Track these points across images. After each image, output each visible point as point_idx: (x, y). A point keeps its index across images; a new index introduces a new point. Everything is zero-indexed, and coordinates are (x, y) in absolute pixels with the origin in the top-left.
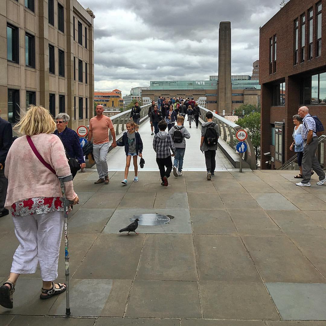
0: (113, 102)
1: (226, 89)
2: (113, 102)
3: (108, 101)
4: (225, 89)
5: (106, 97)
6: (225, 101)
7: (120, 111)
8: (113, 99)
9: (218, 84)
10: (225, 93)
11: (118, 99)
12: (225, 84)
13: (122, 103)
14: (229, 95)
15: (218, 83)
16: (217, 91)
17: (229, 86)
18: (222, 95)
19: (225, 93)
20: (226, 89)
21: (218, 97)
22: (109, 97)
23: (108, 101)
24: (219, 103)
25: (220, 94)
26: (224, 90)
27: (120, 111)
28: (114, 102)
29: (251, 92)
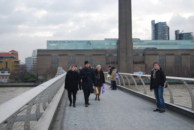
0: (7, 63)
1: (127, 49)
2: (7, 63)
4: (126, 48)
7: (10, 74)
8: (6, 60)
10: (127, 54)
11: (13, 60)
13: (18, 64)
15: (119, 43)
16: (118, 51)
19: (127, 54)
20: (128, 48)
21: (118, 57)
24: (120, 64)
27: (10, 74)
28: (8, 63)
29: (152, 52)
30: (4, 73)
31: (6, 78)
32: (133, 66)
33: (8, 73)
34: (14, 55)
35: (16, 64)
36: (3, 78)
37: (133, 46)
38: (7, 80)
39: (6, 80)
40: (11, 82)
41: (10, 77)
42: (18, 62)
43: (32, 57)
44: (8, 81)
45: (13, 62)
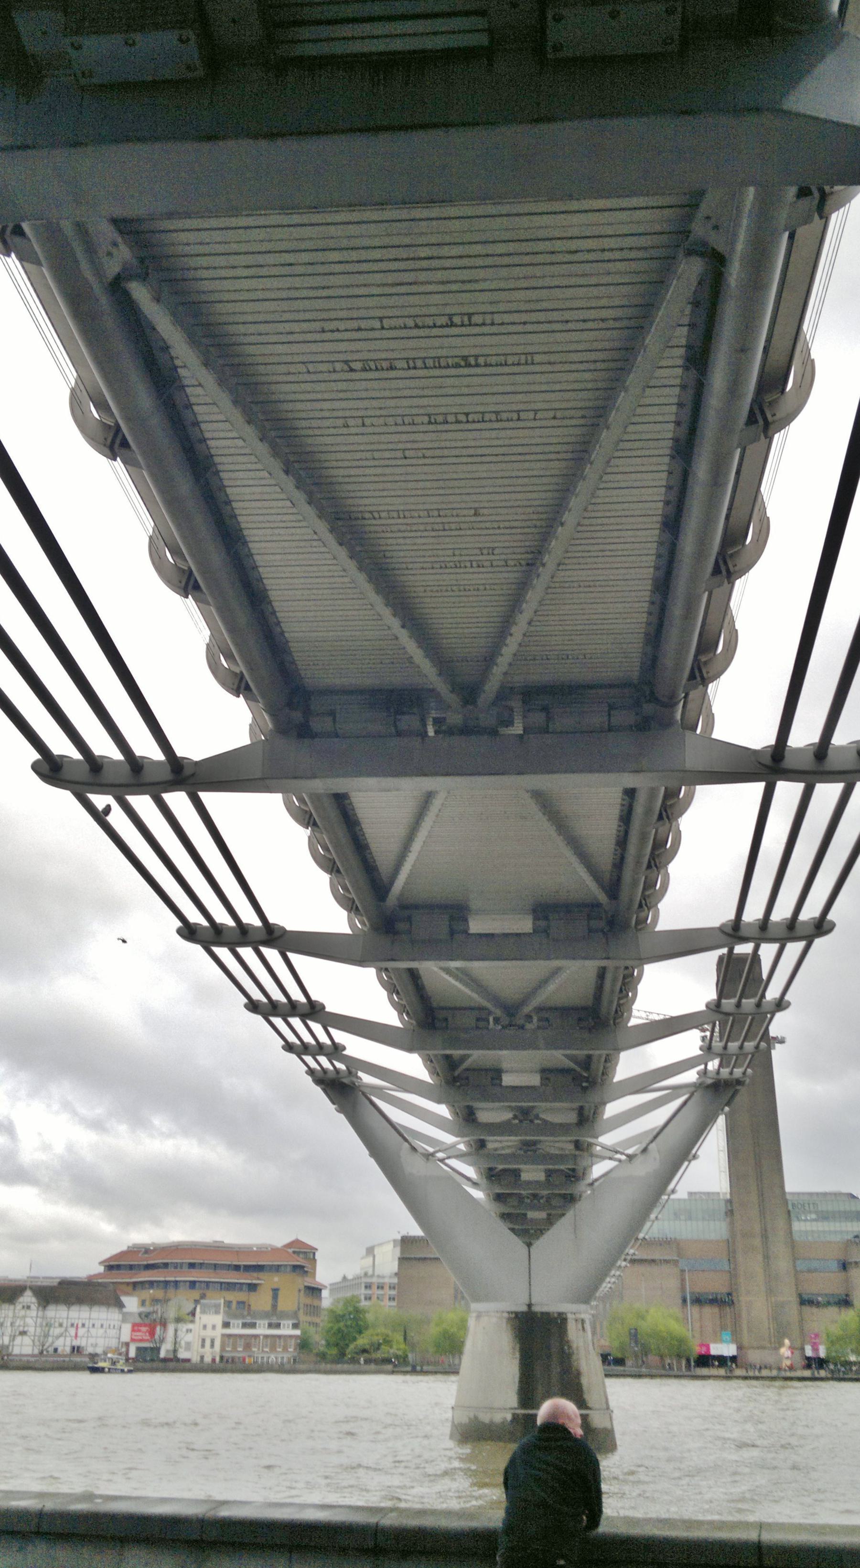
0: (275, 1291)
2: (275, 1291)
3: (253, 1287)
4: (765, 1236)
5: (248, 1268)
6: (770, 1292)
7: (298, 1332)
9: (730, 1213)
10: (766, 1257)
11: (301, 1282)
12: (762, 1213)
14: (782, 1264)
16: (730, 1247)
17: (781, 1223)
18: (751, 1264)
21: (733, 1275)
22: (259, 1268)
23: (253, 1287)
25: (740, 1258)
26: (757, 1242)
27: (298, 1332)
30: (278, 1326)
32: (800, 1314)
33: (295, 1326)
34: (300, 1260)
35: (309, 1301)
37: (797, 1226)
42: (314, 1291)
43: (364, 1280)
45: (300, 1291)
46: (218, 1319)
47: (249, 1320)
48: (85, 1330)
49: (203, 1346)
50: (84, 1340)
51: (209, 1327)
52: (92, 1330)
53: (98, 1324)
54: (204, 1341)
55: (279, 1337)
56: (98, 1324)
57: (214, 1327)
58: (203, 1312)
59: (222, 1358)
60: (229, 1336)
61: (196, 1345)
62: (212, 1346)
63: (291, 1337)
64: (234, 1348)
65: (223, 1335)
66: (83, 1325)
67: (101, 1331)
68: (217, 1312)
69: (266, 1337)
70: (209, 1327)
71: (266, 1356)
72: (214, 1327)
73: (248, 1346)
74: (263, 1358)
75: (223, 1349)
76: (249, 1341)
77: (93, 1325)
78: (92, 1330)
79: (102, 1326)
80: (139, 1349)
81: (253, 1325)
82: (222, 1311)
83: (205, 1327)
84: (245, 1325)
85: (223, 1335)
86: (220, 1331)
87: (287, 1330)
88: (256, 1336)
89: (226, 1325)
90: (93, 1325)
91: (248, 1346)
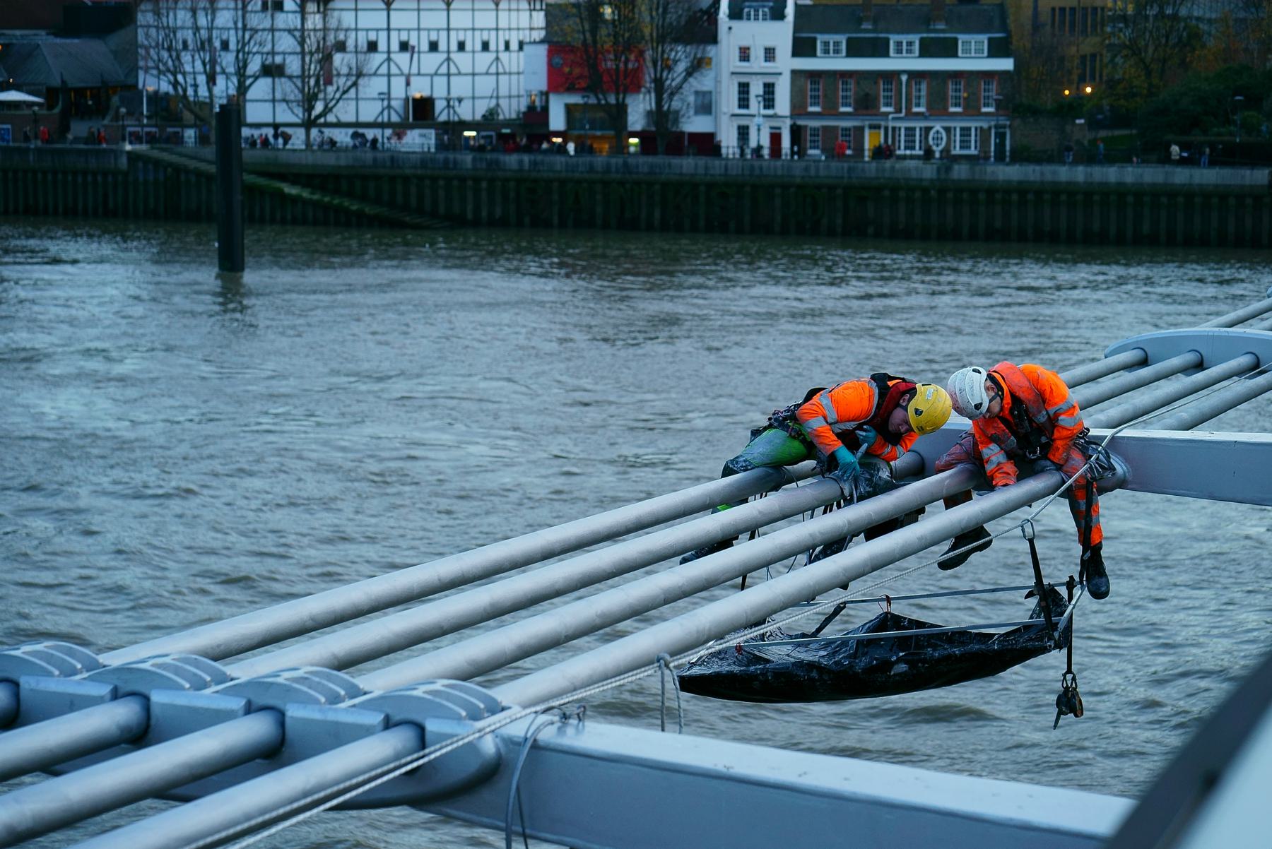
7: (1006, 64)
27: (1006, 64)
30: (949, 50)
31: (971, 109)
33: (996, 50)
36: (937, 108)
38: (973, 125)
39: (965, 132)
40: (1021, 156)
41: (1015, 97)
44: (984, 134)
46: (781, 34)
47: (867, 31)
48: (438, 58)
49: (744, 102)
50: (440, 82)
51: (757, 54)
52: (456, 57)
53: (473, 42)
54: (744, 89)
55: (956, 75)
56: (473, 42)
57: (770, 54)
58: (735, 14)
59: (796, 132)
60: (814, 75)
61: (728, 101)
62: (769, 101)
63: (988, 75)
64: (830, 111)
65: (795, 73)
66: (434, 47)
67: (484, 60)
68: (778, 15)
69: (916, 76)
70: (757, 54)
71: (918, 125)
72: (770, 54)
73: (866, 104)
74: (910, 131)
75: (798, 109)
76: (867, 93)
77: (461, 46)
78: (456, 57)
79: (485, 46)
80: (569, 109)
81: (880, 50)
82: (790, 10)
83: (745, 54)
84: (855, 50)
85: (795, 73)
86: (786, 63)
87: (974, 57)
88: (890, 77)
89: (802, 47)
90: (461, 46)
91: (866, 104)
